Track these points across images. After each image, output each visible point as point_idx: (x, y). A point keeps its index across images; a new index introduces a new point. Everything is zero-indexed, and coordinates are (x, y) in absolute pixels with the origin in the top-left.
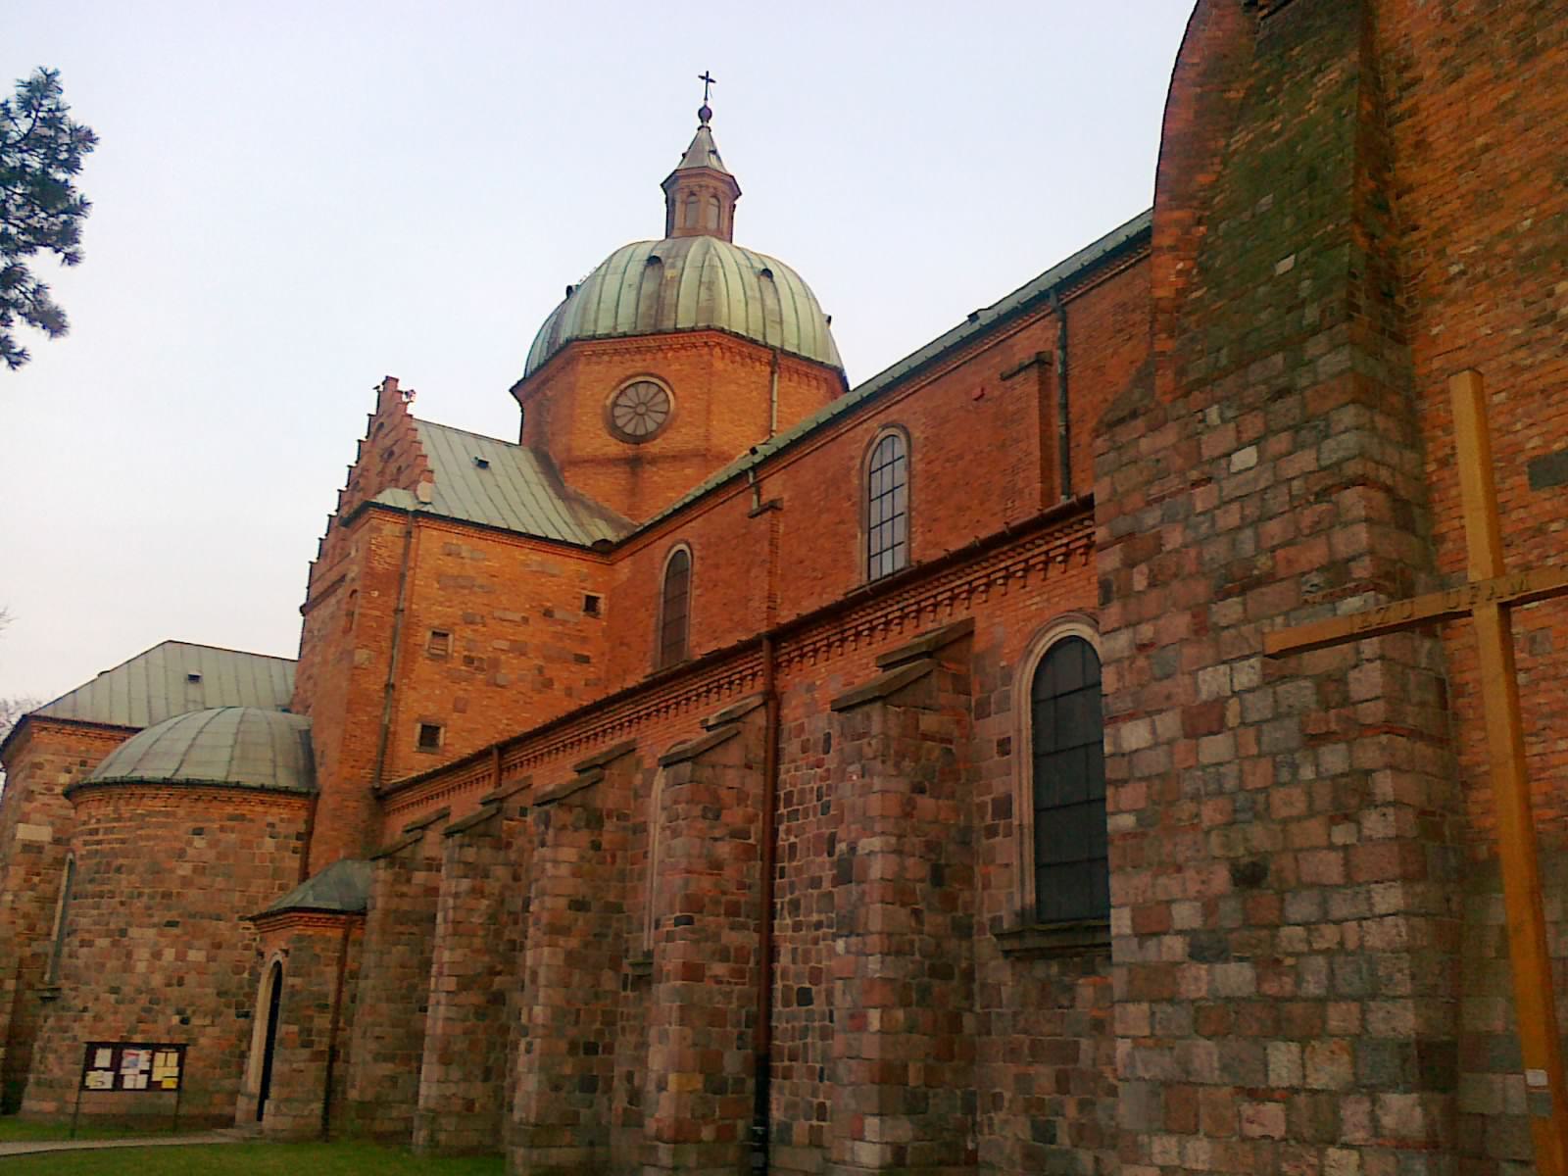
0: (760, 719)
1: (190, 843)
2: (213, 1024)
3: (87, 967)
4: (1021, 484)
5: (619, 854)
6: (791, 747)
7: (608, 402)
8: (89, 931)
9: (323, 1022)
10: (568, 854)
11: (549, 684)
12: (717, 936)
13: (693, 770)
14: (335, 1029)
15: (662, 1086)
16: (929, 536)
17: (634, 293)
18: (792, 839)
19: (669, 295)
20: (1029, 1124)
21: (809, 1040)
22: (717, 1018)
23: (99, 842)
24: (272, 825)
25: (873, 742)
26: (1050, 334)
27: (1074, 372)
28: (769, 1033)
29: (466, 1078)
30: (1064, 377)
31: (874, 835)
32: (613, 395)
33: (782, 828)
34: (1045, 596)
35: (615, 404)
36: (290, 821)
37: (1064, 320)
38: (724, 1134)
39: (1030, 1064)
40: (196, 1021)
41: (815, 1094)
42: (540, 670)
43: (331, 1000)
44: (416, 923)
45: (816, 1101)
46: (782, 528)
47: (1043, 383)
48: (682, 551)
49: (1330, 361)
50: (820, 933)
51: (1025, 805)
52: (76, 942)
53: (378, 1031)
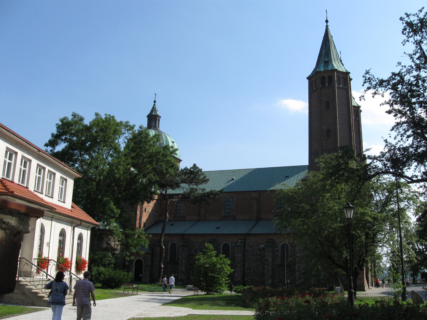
33: (246, 253)
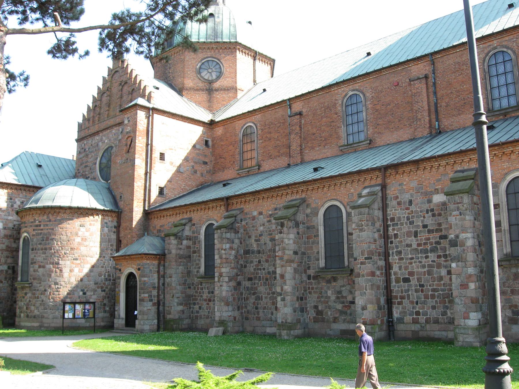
0: (380, 194)
1: (79, 230)
2: (94, 294)
3: (43, 275)
4: (419, 117)
5: (304, 235)
6: (392, 203)
7: (198, 67)
8: (41, 262)
9: (155, 293)
10: (292, 236)
11: (195, 172)
12: (377, 263)
13: (368, 211)
14: (158, 296)
16: (376, 130)
18: (396, 232)
19: (219, 28)
20: (511, 311)
21: (410, 293)
22: (378, 288)
23: (42, 230)
24: (106, 223)
25: (465, 205)
26: (427, 68)
27: (438, 82)
28: (391, 291)
29: (233, 310)
30: (434, 84)
31: (468, 233)
32: (199, 65)
33: (390, 229)
34: (510, 163)
35: (200, 68)
36: (112, 221)
37: (433, 64)
38: (382, 321)
39: (510, 296)
40: (88, 294)
41: (414, 308)
42: (193, 168)
43: (156, 285)
44: (185, 258)
45: (415, 311)
46: (303, 122)
47: (427, 84)
48: (251, 126)
50: (413, 261)
51: (505, 224)
52: (36, 266)
53: (177, 295)
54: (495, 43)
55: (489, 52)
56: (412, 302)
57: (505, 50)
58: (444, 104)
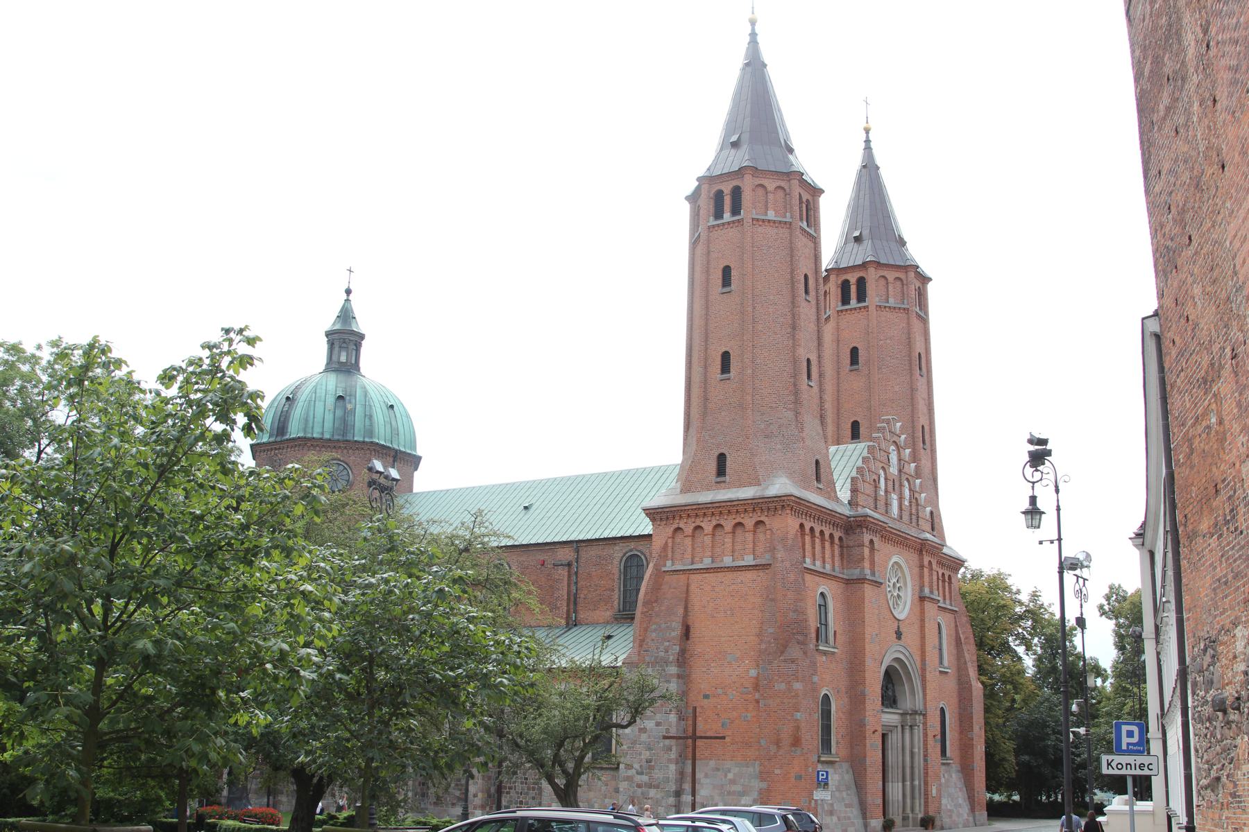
4: (559, 605)
15: (475, 796)
17: (332, 415)
19: (350, 419)
37: (578, 552)
41: (519, 798)
47: (569, 572)
49: (673, 670)
54: (632, 545)
55: (627, 553)
56: (517, 793)
57: (639, 554)
58: (582, 596)
